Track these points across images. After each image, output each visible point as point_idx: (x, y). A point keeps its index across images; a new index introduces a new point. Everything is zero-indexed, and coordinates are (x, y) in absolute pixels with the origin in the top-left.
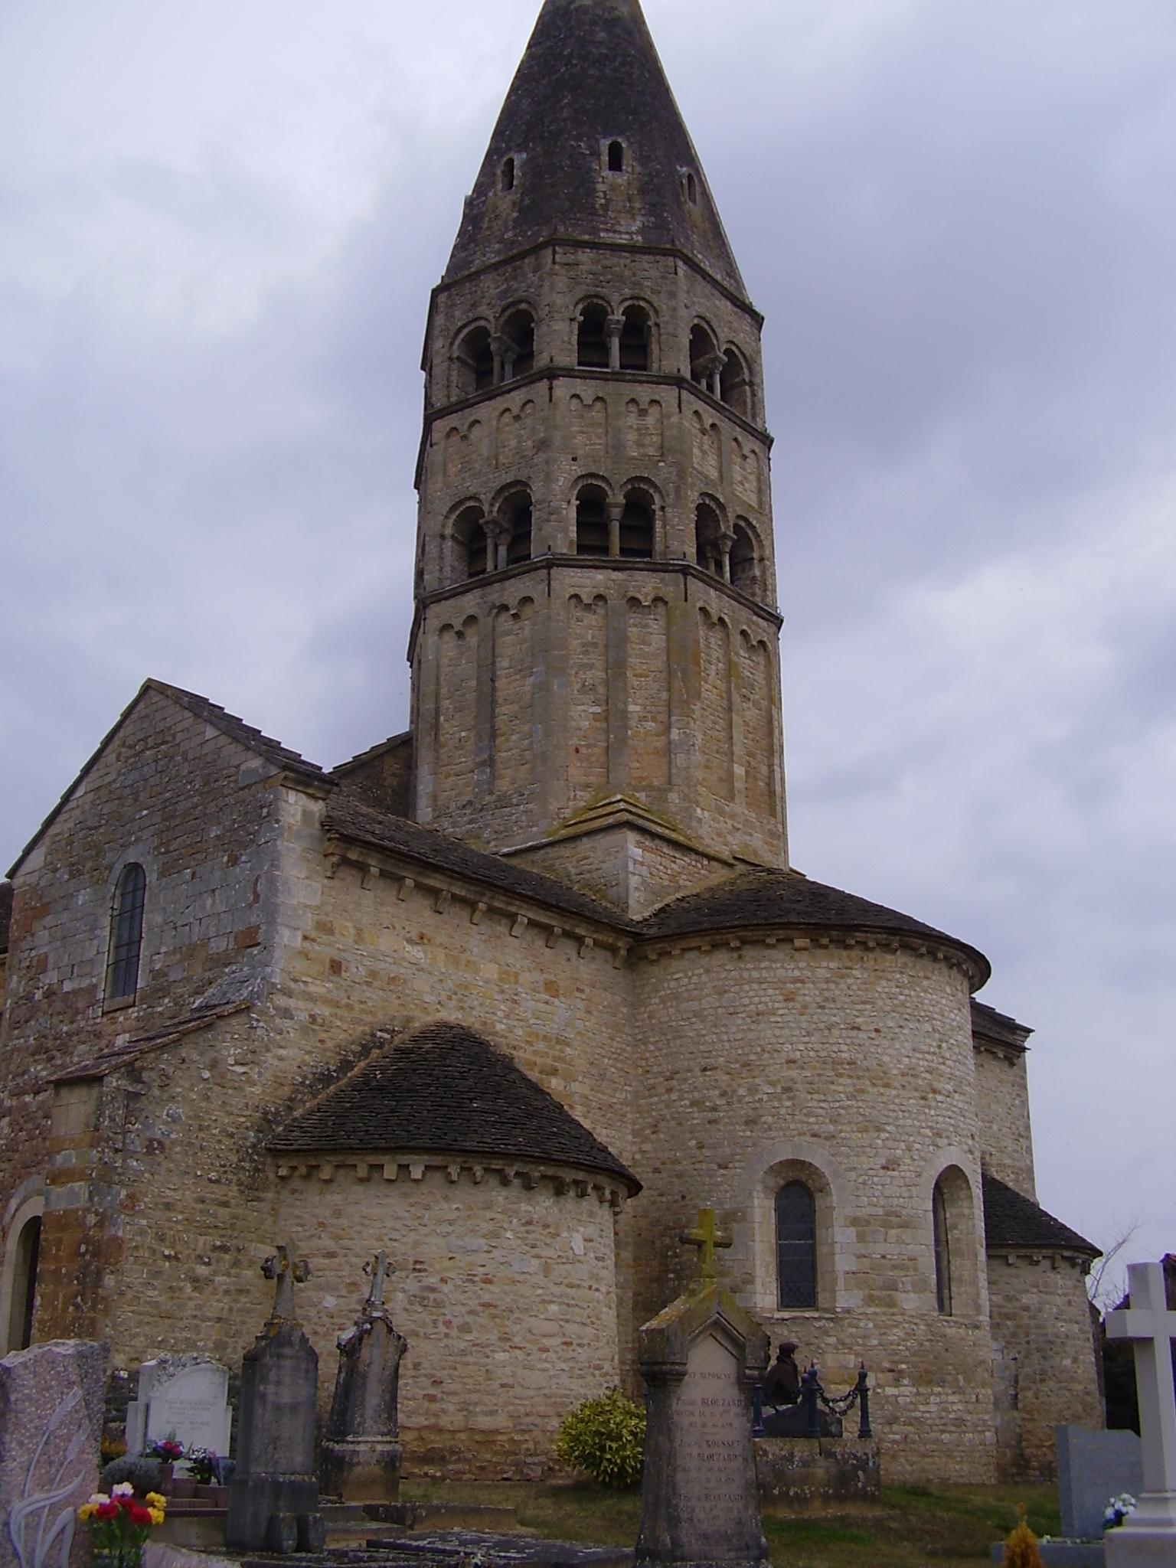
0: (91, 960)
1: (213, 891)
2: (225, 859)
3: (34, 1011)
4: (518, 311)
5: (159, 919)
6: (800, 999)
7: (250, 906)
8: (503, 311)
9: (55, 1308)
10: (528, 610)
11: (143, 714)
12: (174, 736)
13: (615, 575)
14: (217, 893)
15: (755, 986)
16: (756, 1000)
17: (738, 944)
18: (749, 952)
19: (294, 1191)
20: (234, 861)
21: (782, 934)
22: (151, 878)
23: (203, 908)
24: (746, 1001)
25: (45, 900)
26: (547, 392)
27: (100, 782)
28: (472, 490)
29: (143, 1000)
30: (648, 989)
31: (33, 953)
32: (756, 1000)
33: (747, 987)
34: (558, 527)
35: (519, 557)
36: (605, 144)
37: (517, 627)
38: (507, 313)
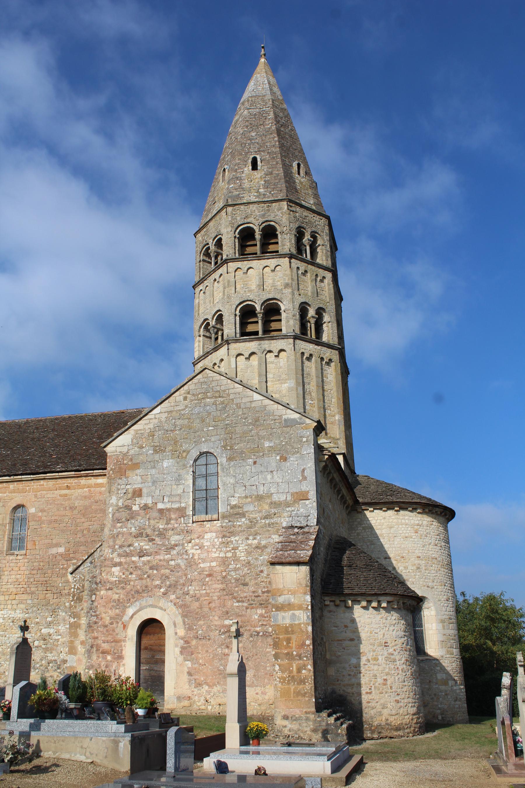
0: (179, 495)
1: (272, 472)
2: (278, 458)
3: (132, 516)
4: (270, 225)
5: (232, 481)
6: (419, 532)
7: (301, 481)
8: (262, 223)
9: (291, 672)
10: (282, 354)
11: (202, 380)
12: (229, 395)
13: (316, 347)
14: (275, 473)
15: (404, 526)
16: (405, 531)
17: (398, 509)
18: (402, 512)
19: (330, 611)
20: (284, 459)
21: (415, 506)
22: (223, 460)
23: (265, 479)
24: (401, 532)
25: (134, 461)
26: (288, 263)
27: (171, 409)
28: (251, 297)
29: (224, 517)
30: (356, 523)
31: (128, 487)
32: (405, 531)
33: (400, 526)
34: (288, 322)
35: (268, 331)
36: (295, 164)
37: (275, 361)
38: (264, 224)
